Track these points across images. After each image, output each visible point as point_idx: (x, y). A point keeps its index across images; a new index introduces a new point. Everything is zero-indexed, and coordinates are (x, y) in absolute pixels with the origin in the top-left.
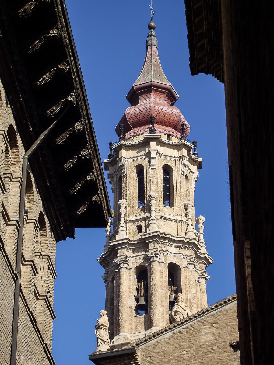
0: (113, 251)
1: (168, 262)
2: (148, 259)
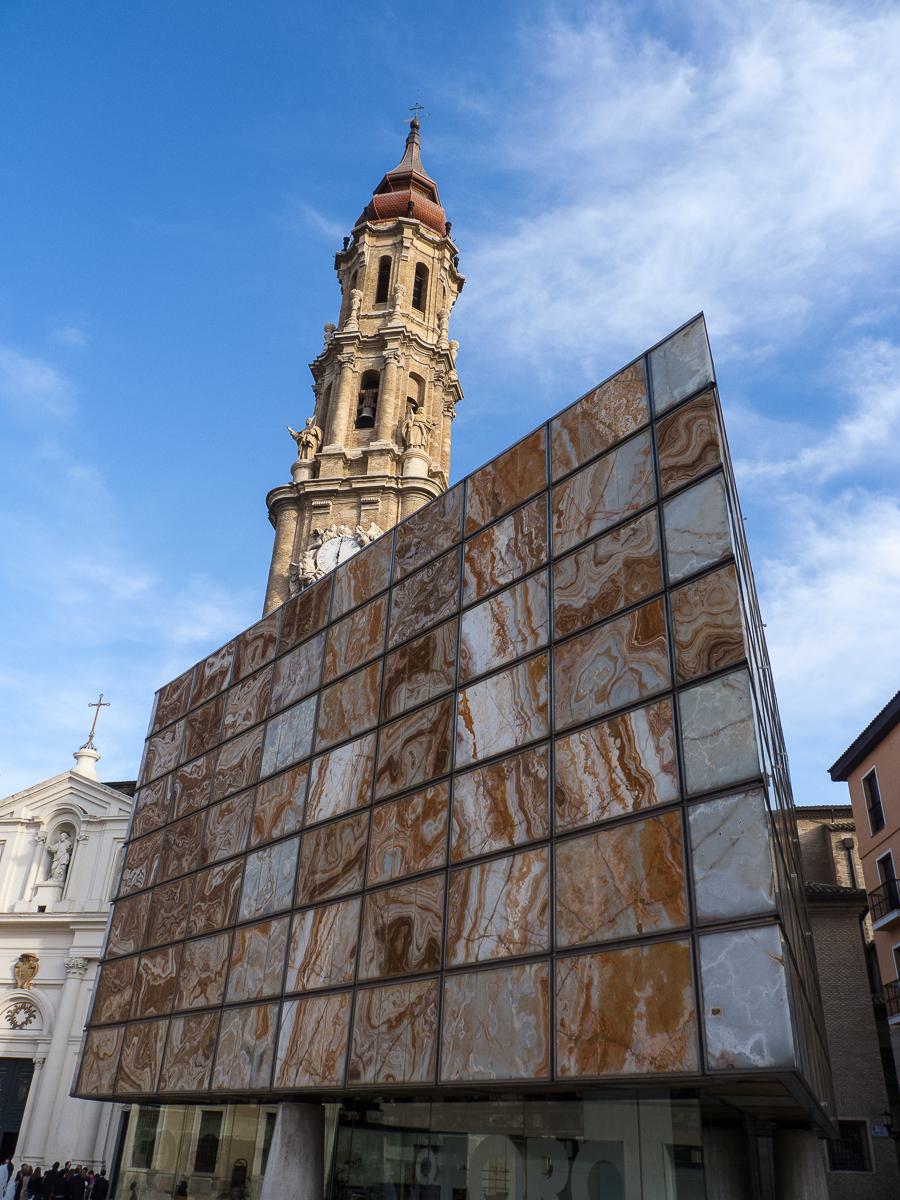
0: (336, 347)
1: (410, 370)
2: (385, 361)
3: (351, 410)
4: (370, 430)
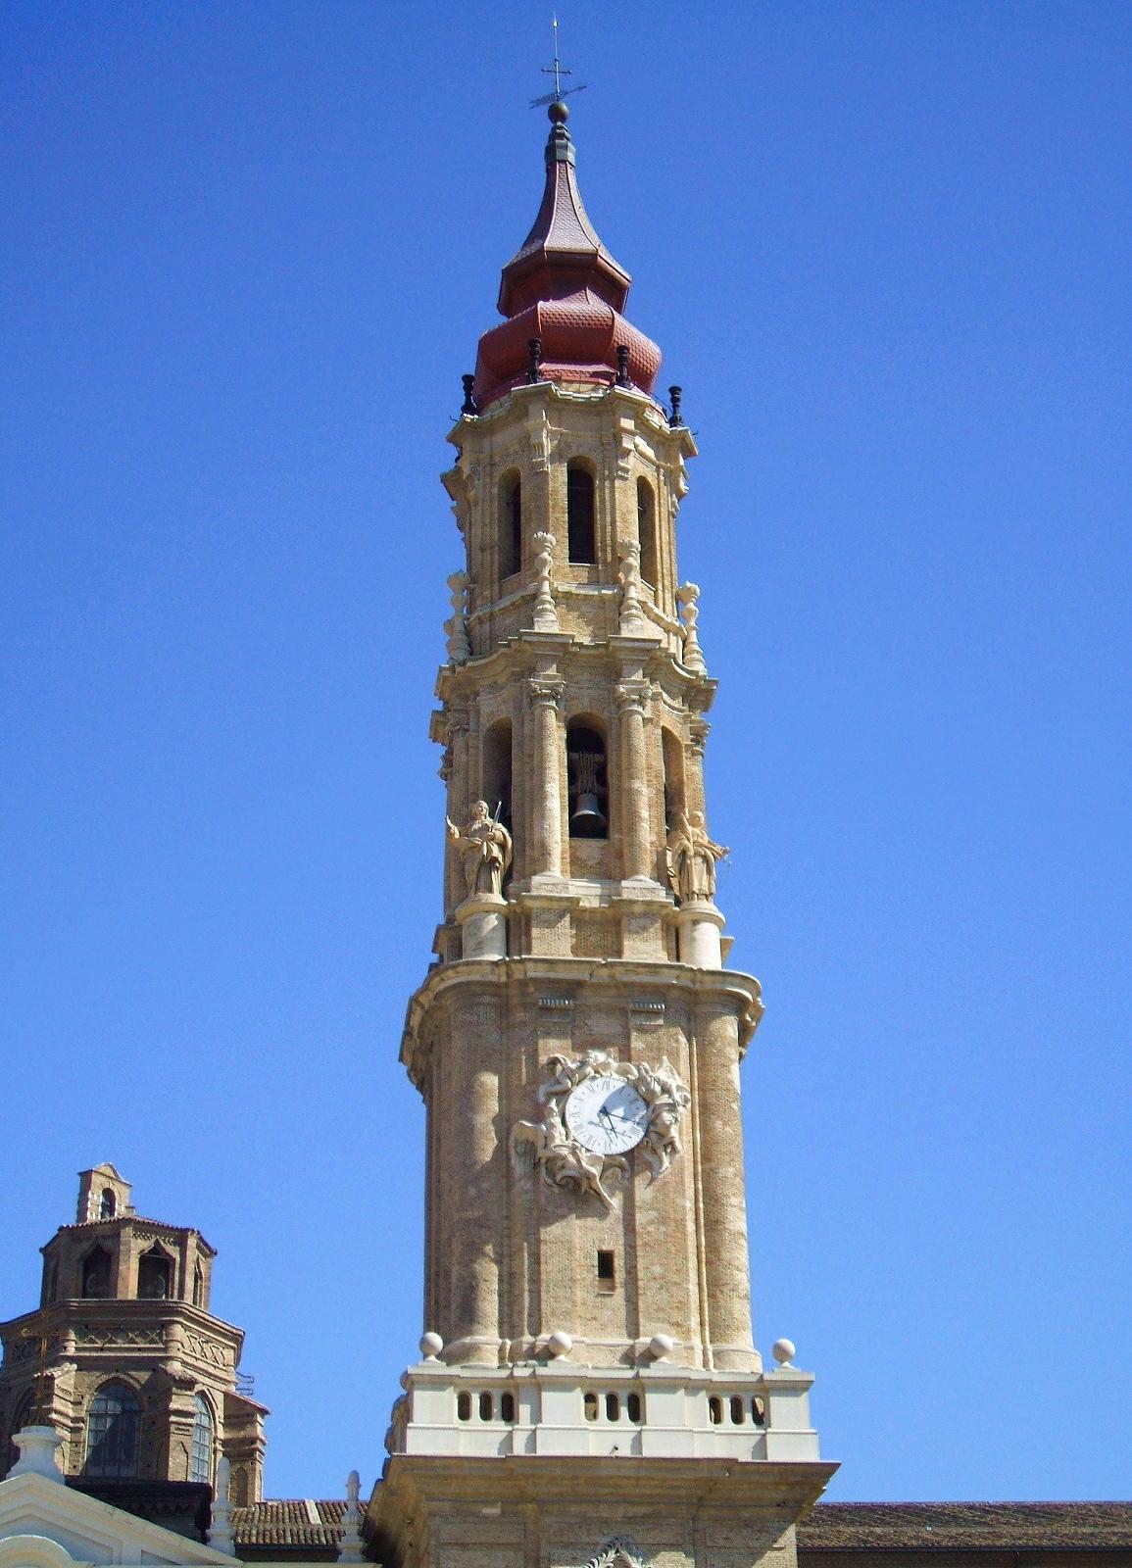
4: (602, 843)
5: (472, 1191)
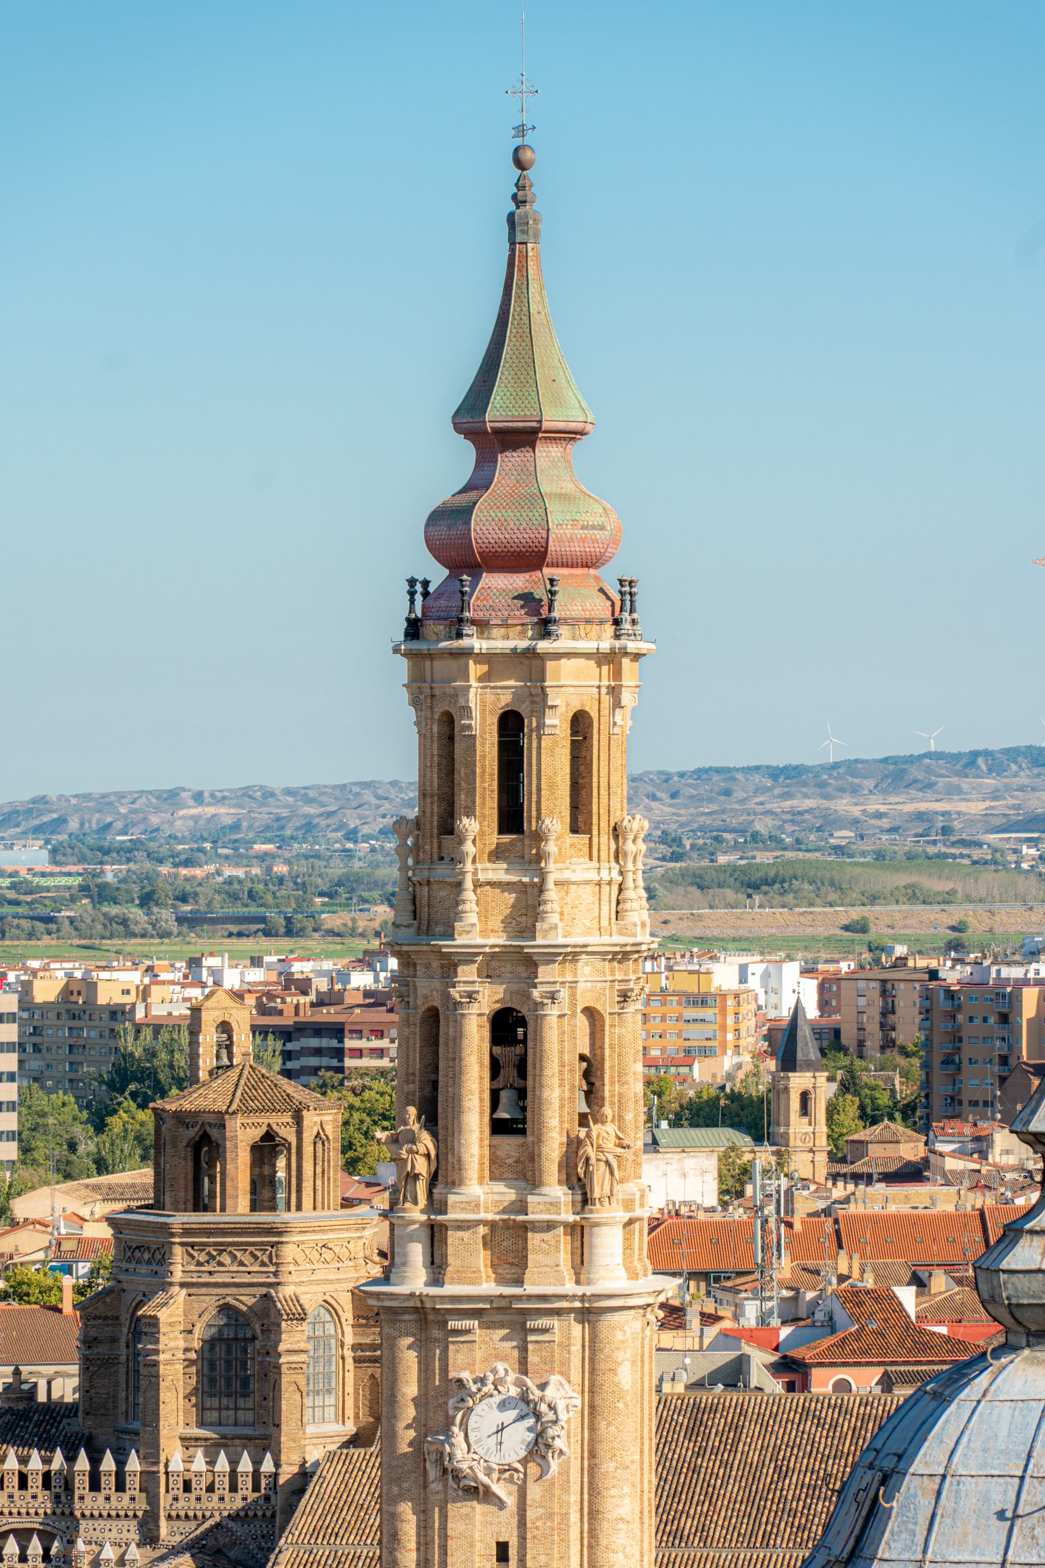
3: (481, 1100)
5: (395, 1490)
